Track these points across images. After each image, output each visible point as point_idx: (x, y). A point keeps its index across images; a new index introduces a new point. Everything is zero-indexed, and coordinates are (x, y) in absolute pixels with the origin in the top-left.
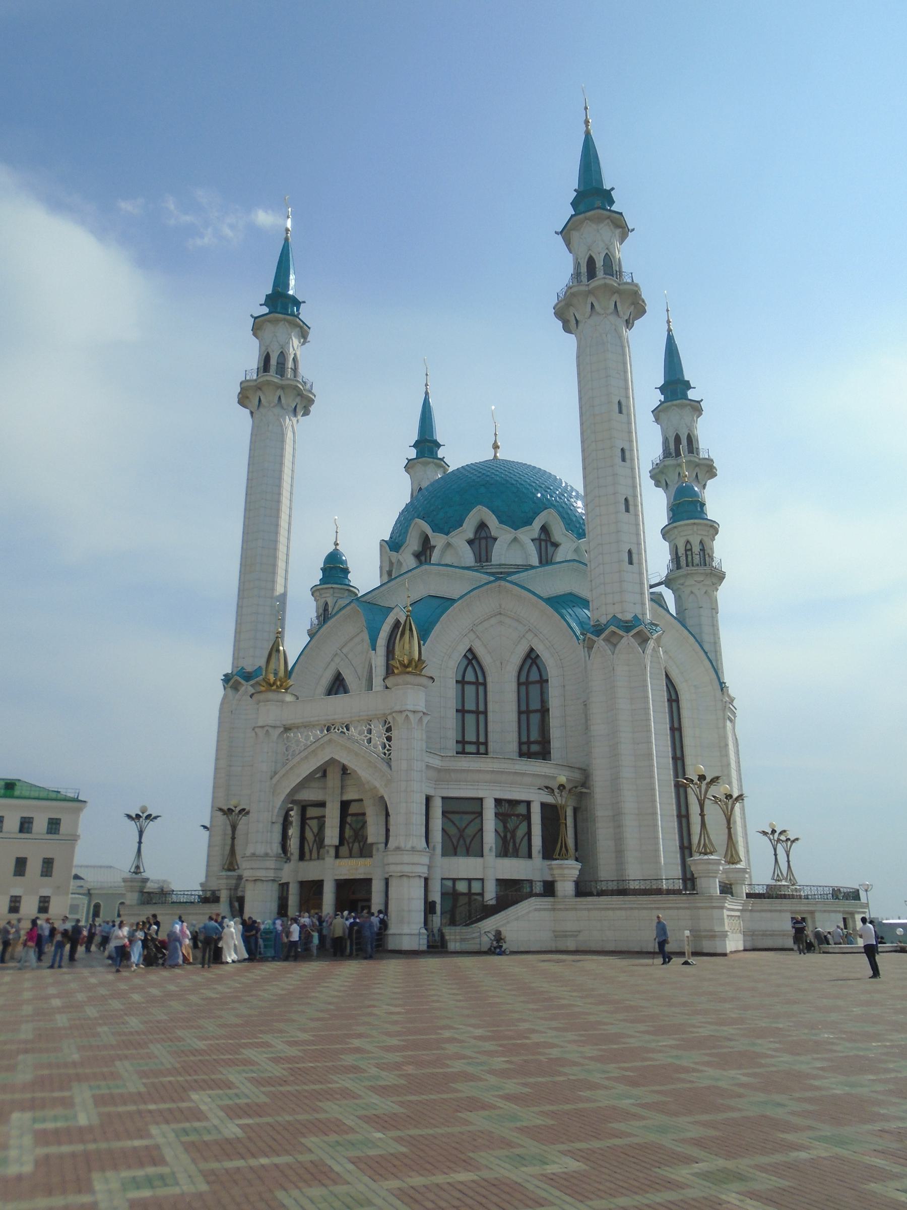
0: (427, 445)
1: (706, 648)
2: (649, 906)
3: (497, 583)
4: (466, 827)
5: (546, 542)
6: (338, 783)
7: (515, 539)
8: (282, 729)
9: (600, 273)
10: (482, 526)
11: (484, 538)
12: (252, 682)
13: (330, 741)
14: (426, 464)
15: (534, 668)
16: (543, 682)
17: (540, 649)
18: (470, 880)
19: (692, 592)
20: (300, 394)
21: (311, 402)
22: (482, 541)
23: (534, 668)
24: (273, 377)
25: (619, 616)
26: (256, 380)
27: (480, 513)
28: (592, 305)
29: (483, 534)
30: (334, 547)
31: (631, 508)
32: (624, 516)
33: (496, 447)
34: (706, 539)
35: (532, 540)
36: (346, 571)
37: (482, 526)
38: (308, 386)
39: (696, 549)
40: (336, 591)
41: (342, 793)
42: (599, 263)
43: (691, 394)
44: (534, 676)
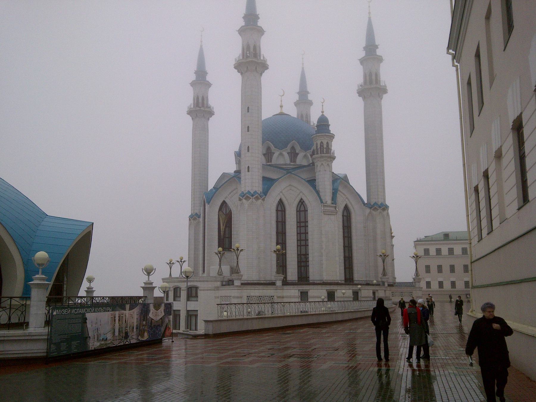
33: (281, 107)
34: (323, 141)
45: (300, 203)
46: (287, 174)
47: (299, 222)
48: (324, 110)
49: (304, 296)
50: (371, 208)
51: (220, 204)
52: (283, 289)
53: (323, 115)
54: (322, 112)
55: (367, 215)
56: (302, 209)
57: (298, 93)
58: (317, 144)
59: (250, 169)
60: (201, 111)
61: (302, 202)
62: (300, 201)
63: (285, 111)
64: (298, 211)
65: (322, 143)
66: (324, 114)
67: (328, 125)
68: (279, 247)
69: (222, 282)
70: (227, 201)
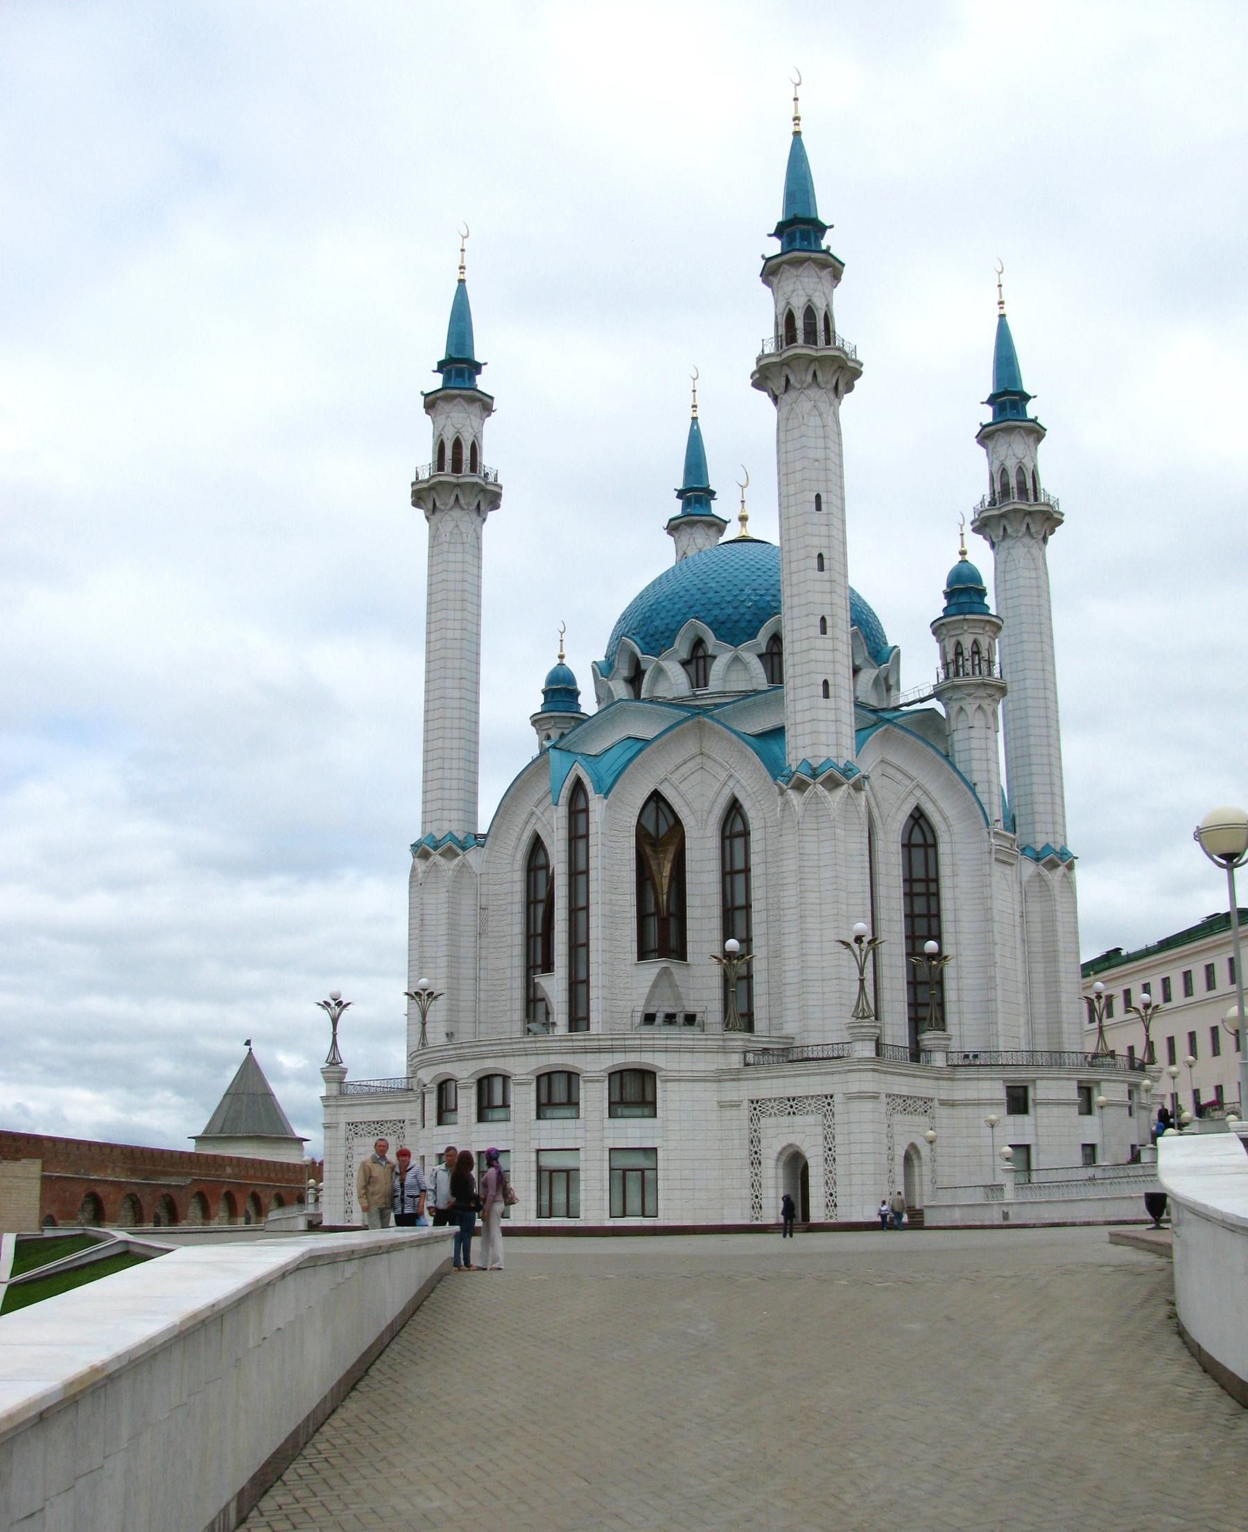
0: (696, 494)
1: (976, 777)
7: (737, 659)
12: (440, 850)
14: (692, 524)
15: (739, 820)
16: (746, 834)
19: (961, 709)
20: (483, 490)
22: (697, 661)
23: (739, 820)
24: (447, 476)
25: (810, 761)
26: (428, 481)
28: (788, 380)
29: (701, 653)
30: (558, 661)
31: (829, 630)
34: (980, 638)
35: (760, 656)
37: (699, 643)
38: (491, 479)
39: (967, 654)
40: (558, 720)
43: (1031, 410)
44: (739, 827)
45: (912, 822)
46: (875, 725)
47: (909, 880)
48: (966, 548)
49: (1018, 1102)
50: (1037, 860)
51: (641, 803)
52: (952, 1079)
53: (964, 561)
54: (963, 553)
55: (1025, 879)
56: (917, 838)
57: (681, 494)
58: (958, 644)
59: (831, 689)
60: (456, 488)
61: (918, 818)
62: (911, 816)
63: (753, 531)
64: (908, 846)
65: (975, 642)
66: (967, 557)
67: (982, 593)
68: (931, 946)
69: (745, 1053)
70: (669, 793)
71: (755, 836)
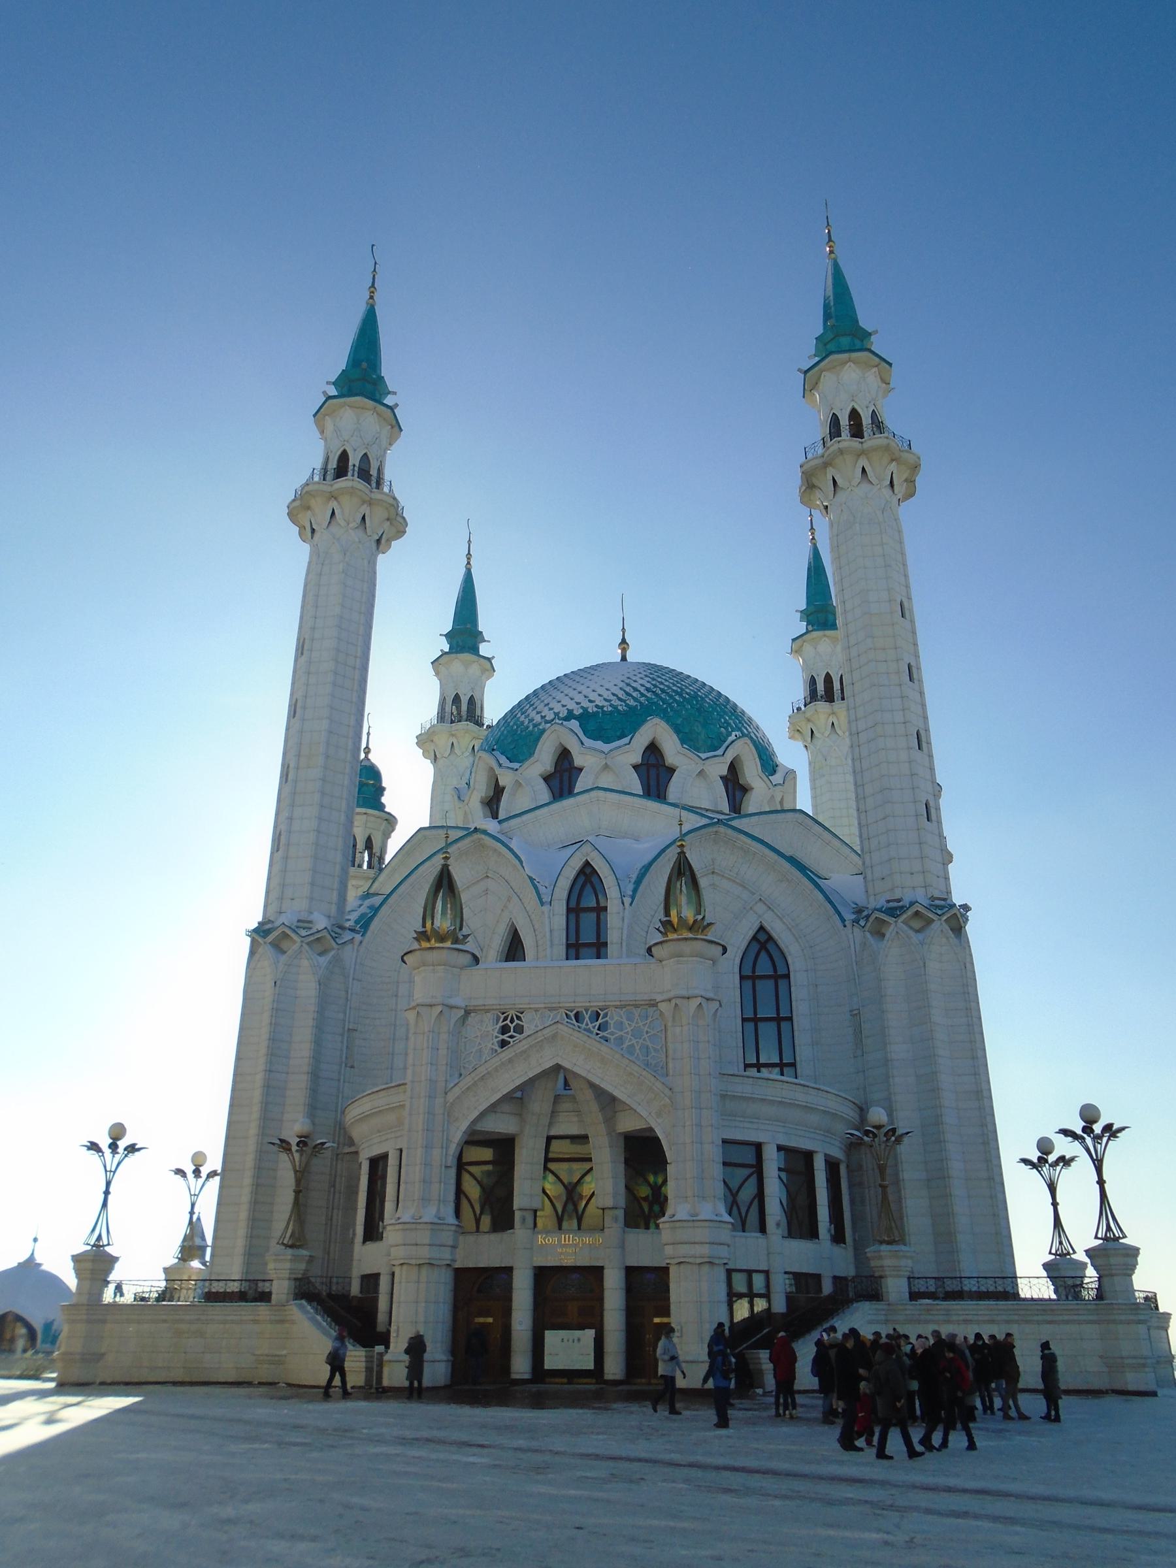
2: (1036, 1318)
3: (714, 829)
4: (740, 1187)
5: (735, 785)
6: (547, 1107)
8: (462, 1012)
9: (867, 431)
10: (653, 749)
11: (653, 765)
13: (554, 1036)
17: (777, 929)
18: (750, 1273)
21: (401, 532)
27: (656, 729)
29: (652, 761)
31: (924, 745)
32: (917, 755)
36: (381, 790)
37: (653, 749)
41: (550, 1124)
42: (866, 420)
71: (798, 977)
